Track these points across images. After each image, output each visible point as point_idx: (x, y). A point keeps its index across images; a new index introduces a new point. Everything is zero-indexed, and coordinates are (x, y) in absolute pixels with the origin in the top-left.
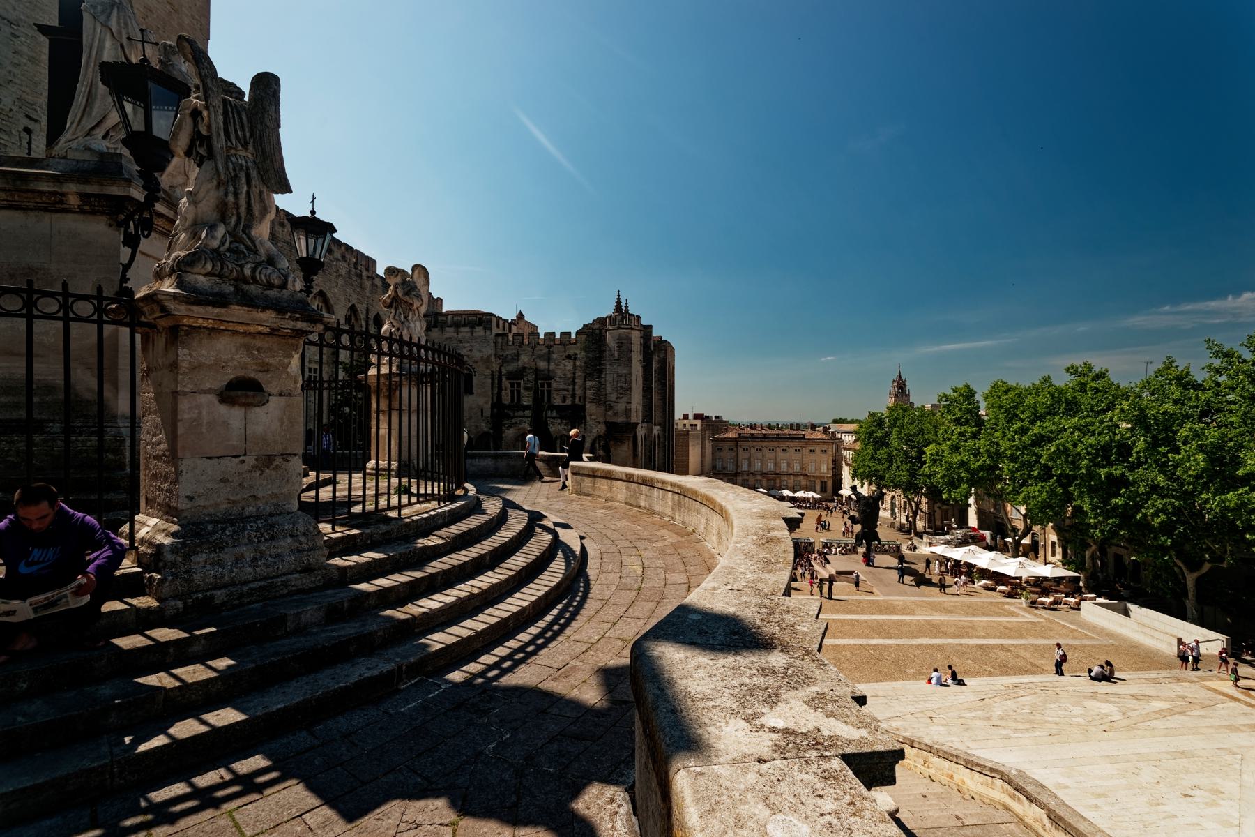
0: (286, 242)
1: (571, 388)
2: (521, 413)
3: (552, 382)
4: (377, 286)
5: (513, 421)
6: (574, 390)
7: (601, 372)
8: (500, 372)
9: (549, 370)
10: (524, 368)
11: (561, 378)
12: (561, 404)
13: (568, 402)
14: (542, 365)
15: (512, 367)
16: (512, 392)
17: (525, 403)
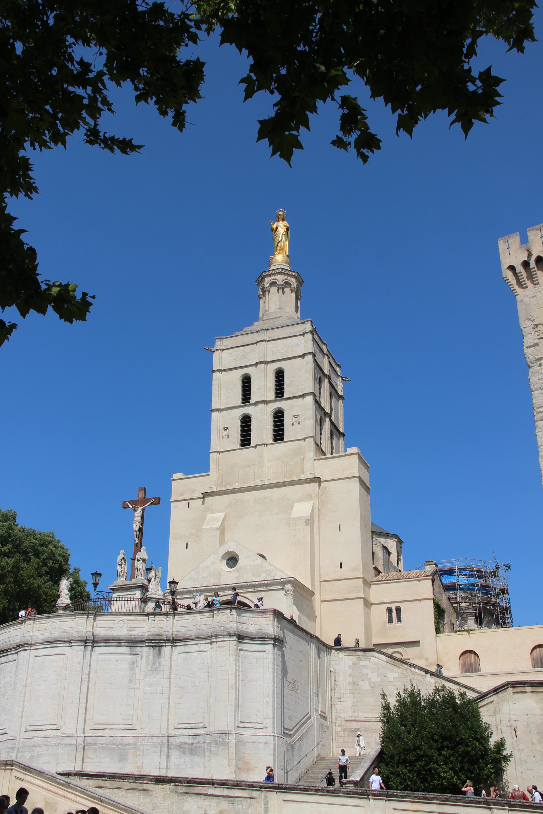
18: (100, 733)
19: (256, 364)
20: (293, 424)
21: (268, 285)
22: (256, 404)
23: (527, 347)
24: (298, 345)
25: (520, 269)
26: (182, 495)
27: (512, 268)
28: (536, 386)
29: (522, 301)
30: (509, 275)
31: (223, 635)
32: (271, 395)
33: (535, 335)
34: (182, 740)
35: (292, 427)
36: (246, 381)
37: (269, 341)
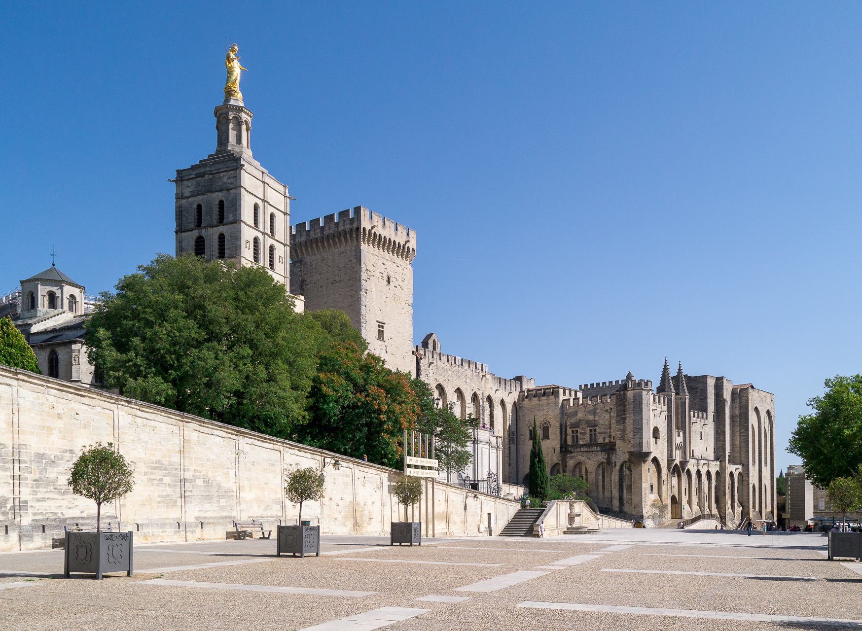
1: (608, 431)
2: (579, 450)
3: (597, 428)
4: (488, 379)
5: (573, 455)
6: (610, 432)
7: (625, 419)
8: (566, 424)
9: (595, 421)
10: (580, 420)
11: (602, 425)
12: (603, 442)
13: (607, 441)
14: (591, 417)
15: (573, 420)
16: (573, 436)
17: (581, 443)
23: (363, 280)
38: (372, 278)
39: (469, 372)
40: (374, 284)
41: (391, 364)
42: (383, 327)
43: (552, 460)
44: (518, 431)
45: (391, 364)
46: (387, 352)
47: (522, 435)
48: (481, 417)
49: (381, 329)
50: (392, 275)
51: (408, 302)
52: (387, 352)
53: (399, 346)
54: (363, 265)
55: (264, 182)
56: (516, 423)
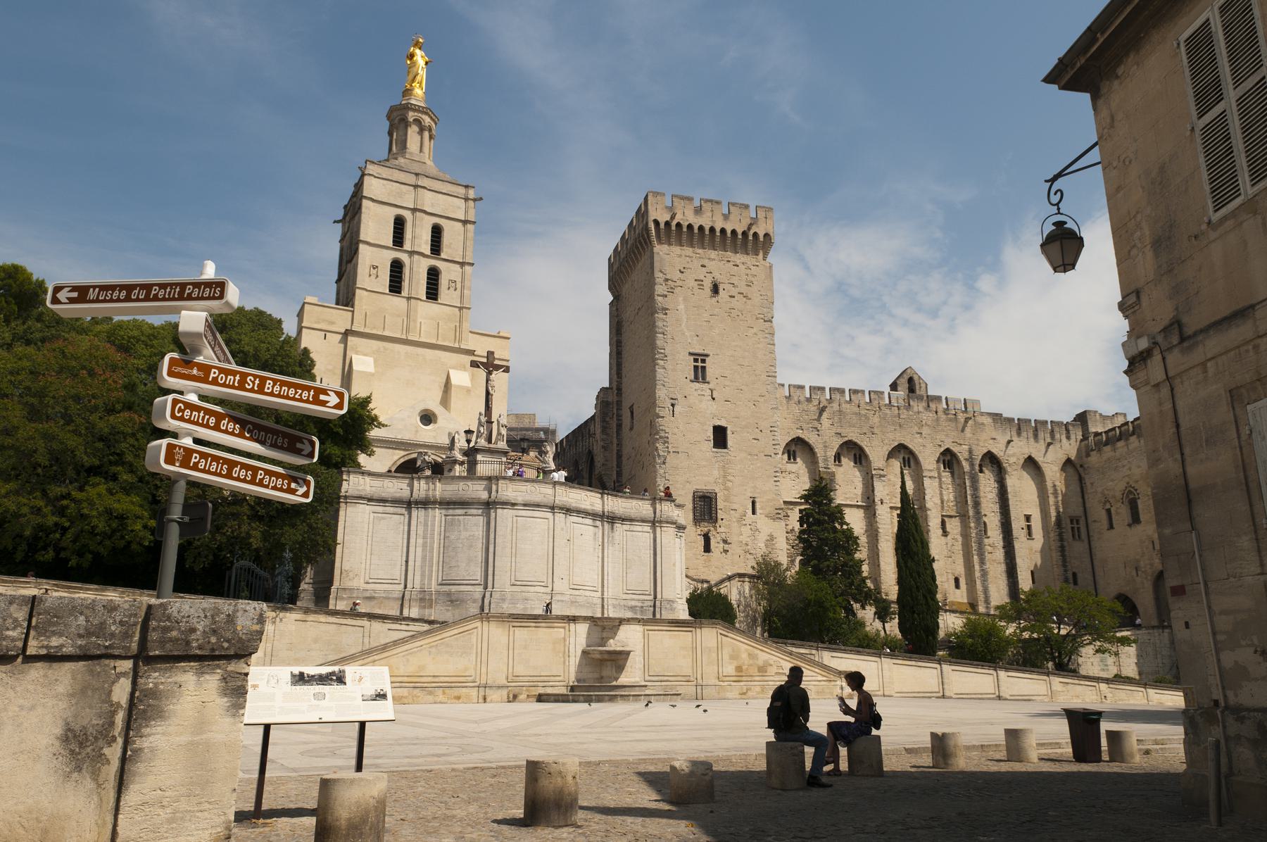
0: (856, 414)
18: (577, 592)
19: (414, 210)
20: (449, 288)
21: (411, 120)
22: (412, 253)
23: (658, 295)
24: (459, 208)
25: (662, 226)
26: (318, 322)
27: (656, 222)
28: (660, 330)
29: (658, 253)
30: (652, 226)
31: (668, 523)
32: (427, 249)
33: (665, 288)
34: (633, 603)
35: (447, 292)
36: (399, 224)
37: (430, 190)
38: (677, 290)
39: (927, 417)
40: (681, 299)
41: (725, 418)
42: (703, 361)
43: (1152, 565)
44: (1088, 515)
45: (725, 418)
46: (714, 399)
47: (1095, 521)
48: (968, 492)
49: (700, 364)
50: (719, 278)
51: (762, 316)
52: (714, 399)
53: (742, 387)
54: (657, 274)
55: (416, 186)
56: (1080, 500)
